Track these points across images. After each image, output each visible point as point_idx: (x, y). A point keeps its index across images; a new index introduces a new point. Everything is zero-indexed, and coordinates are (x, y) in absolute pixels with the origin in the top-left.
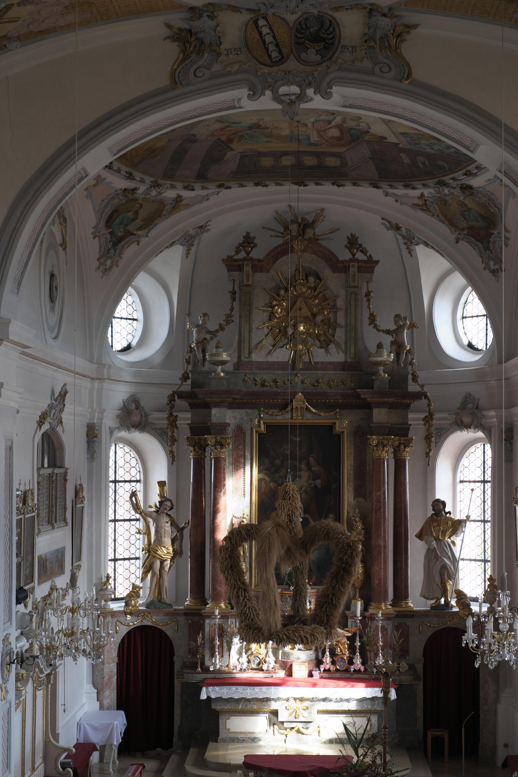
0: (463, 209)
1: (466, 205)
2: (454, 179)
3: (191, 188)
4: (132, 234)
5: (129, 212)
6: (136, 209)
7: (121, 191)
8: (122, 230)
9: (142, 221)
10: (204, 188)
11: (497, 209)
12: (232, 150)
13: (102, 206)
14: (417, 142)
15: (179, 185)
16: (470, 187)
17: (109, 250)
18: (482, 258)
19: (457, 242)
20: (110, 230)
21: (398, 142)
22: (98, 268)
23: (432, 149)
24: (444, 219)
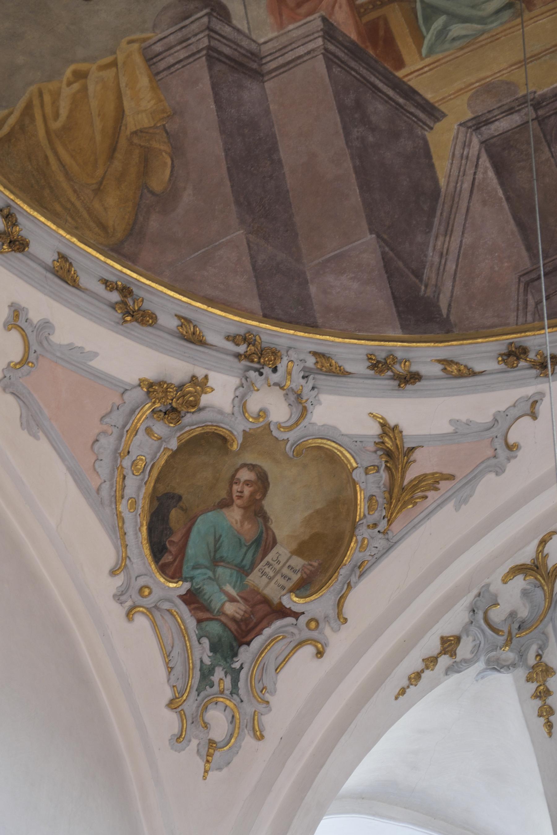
3: (399, 369)
4: (283, 612)
5: (226, 504)
6: (247, 491)
7: (140, 394)
8: (229, 588)
9: (299, 552)
10: (457, 372)
12: (433, 112)
13: (104, 469)
15: (351, 352)
17: (206, 674)
20: (182, 587)
22: (179, 739)
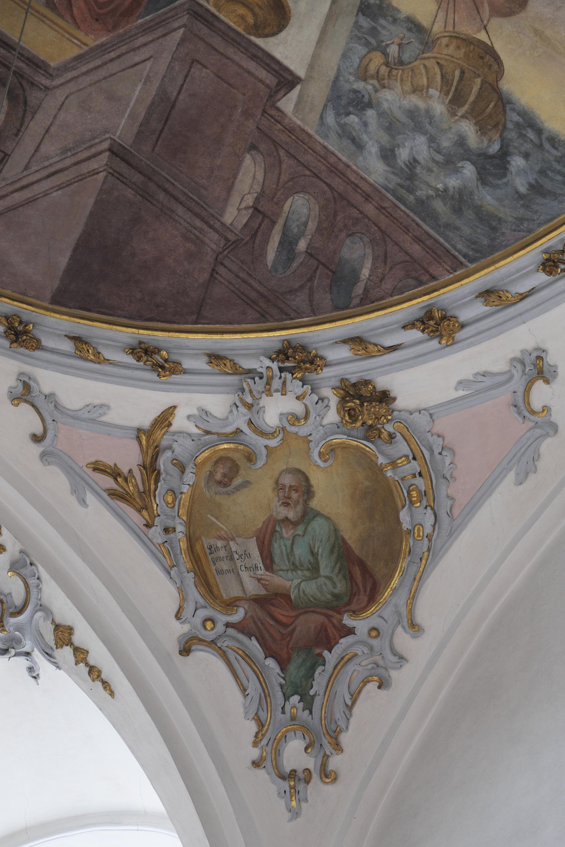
0: (283, 512)
1: (307, 490)
2: (357, 341)
11: (429, 519)
14: (366, 87)
16: (385, 397)
18: (261, 724)
19: (185, 651)
21: (301, 72)
23: (388, 155)
24: (184, 545)
